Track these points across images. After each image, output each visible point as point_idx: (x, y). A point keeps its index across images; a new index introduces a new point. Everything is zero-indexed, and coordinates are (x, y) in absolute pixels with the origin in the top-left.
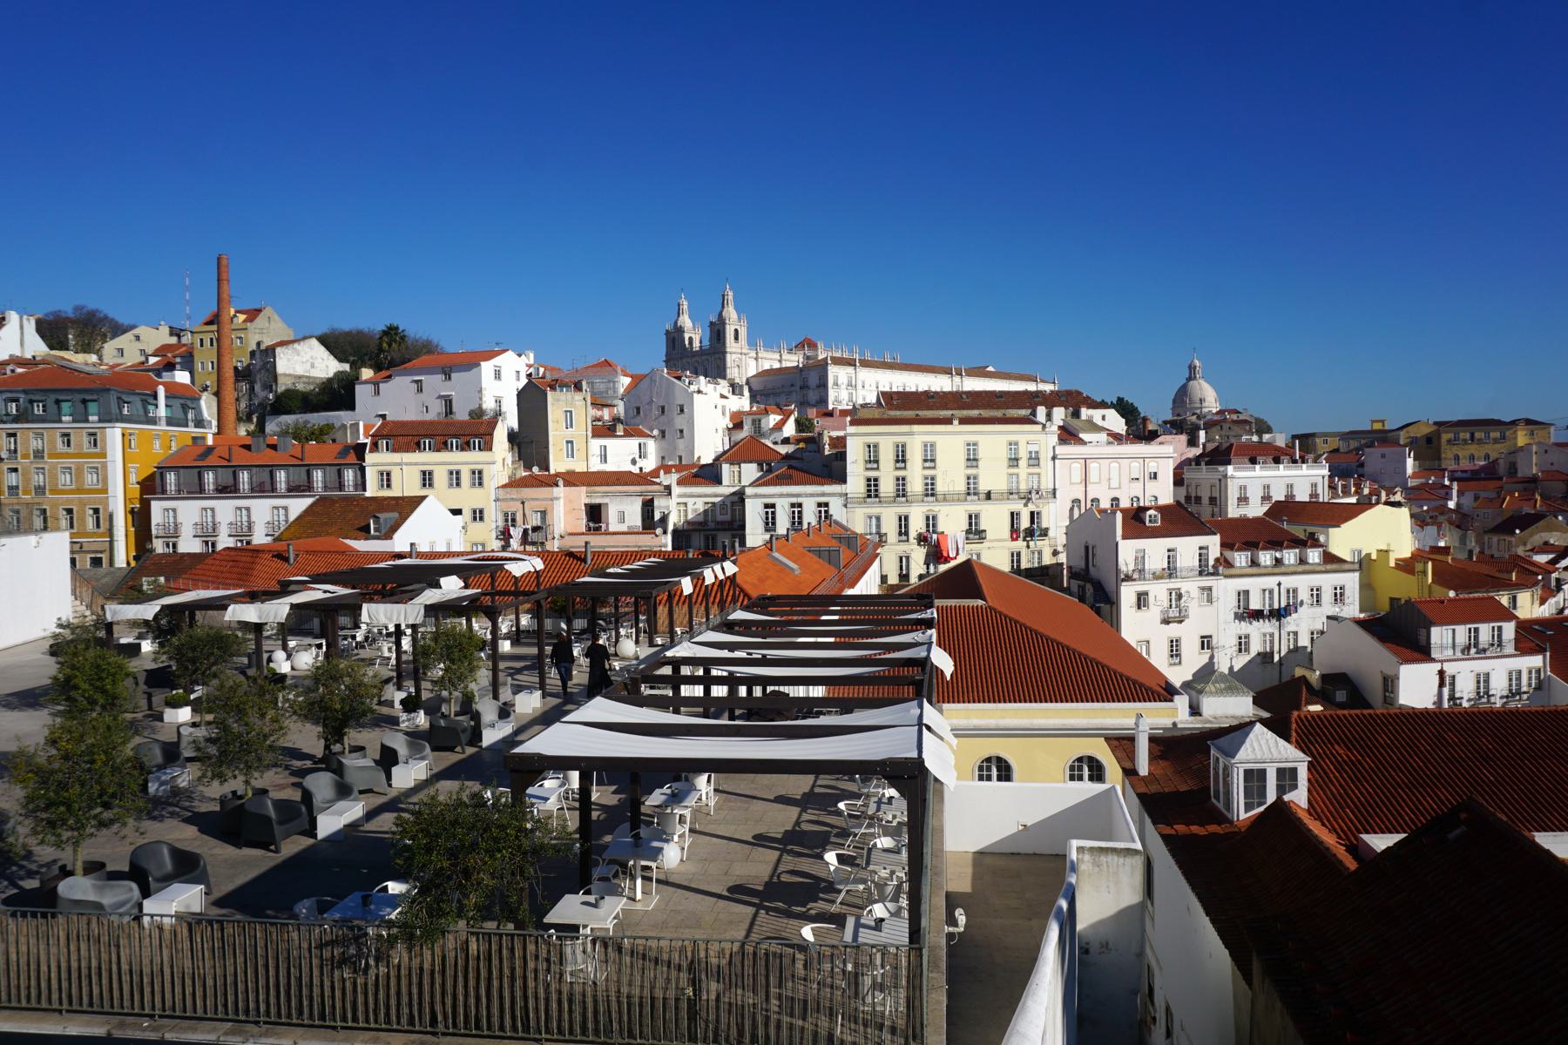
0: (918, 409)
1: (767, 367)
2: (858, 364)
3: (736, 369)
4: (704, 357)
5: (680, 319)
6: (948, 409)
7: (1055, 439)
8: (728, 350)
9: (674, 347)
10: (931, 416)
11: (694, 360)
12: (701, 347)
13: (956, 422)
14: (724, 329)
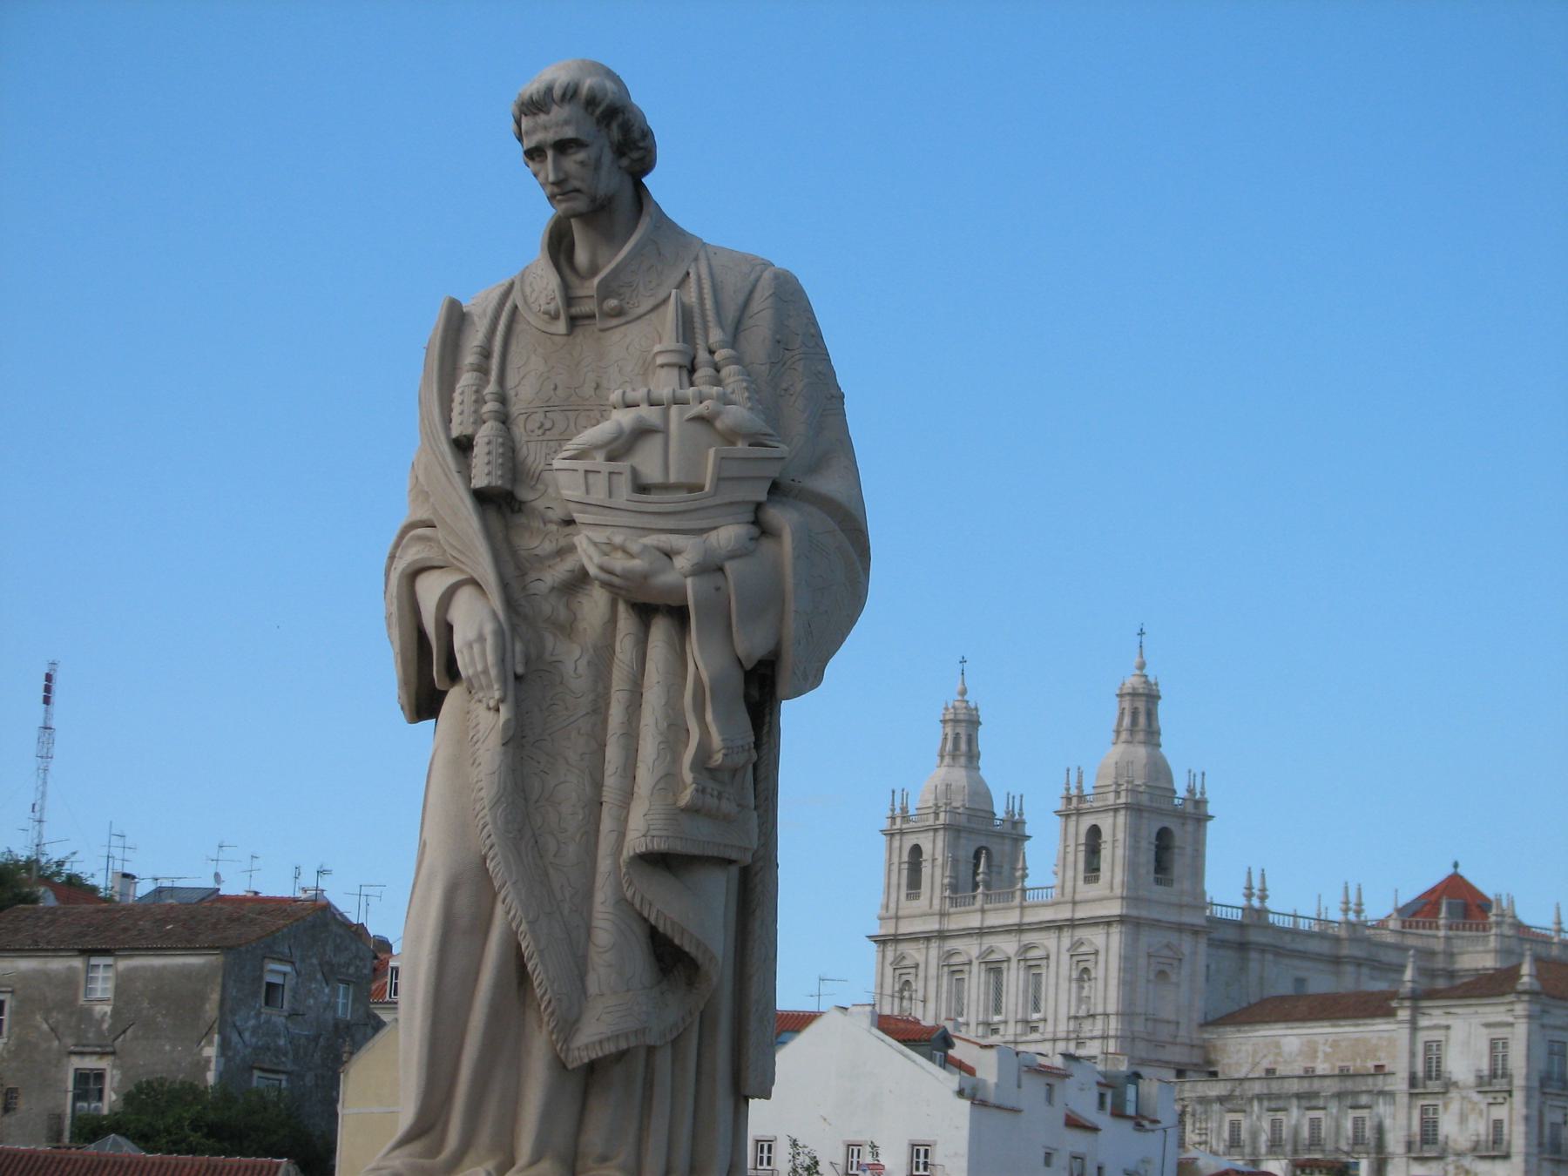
4: (1028, 938)
9: (914, 882)
11: (989, 941)
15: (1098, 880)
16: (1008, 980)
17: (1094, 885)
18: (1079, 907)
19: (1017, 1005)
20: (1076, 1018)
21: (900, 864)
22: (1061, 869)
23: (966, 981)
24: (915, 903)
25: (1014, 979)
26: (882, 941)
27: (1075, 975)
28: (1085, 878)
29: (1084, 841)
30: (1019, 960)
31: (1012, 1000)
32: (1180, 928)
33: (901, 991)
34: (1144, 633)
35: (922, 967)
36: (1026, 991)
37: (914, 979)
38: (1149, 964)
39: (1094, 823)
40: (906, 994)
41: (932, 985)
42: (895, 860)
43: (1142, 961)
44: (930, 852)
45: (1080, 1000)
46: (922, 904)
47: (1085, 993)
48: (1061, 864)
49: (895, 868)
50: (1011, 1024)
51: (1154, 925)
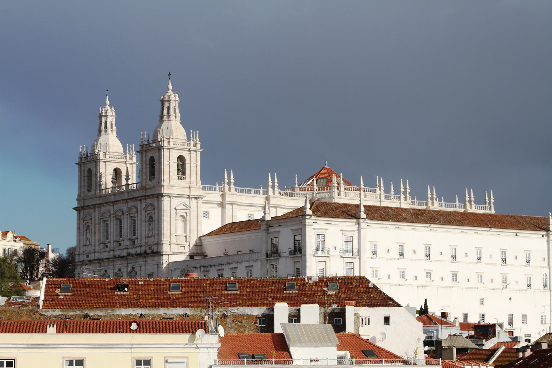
0: (91, 308)
1: (241, 216)
2: (363, 215)
3: (180, 223)
4: (131, 204)
5: (102, 139)
6: (138, 307)
7: (214, 355)
8: (165, 191)
10: (114, 319)
11: (117, 207)
12: (127, 185)
13: (51, 330)
14: (160, 157)
15: (154, 179)
16: (124, 223)
17: (153, 181)
18: (148, 191)
19: (127, 233)
20: (148, 237)
21: (84, 177)
22: (141, 175)
23: (109, 224)
24: (90, 194)
25: (126, 222)
26: (77, 209)
27: (147, 219)
28: (150, 178)
29: (148, 163)
30: (127, 215)
31: (126, 231)
32: (189, 197)
33: (86, 230)
34: (171, 75)
35: (93, 219)
36: (130, 227)
37: (90, 224)
38: (176, 213)
39: (152, 155)
40: (88, 231)
41: (97, 226)
42: (83, 175)
43: (173, 211)
44: (94, 171)
45: (150, 230)
46: (93, 193)
47: (151, 227)
48: (141, 173)
49: (82, 178)
50: (125, 241)
51: (177, 196)
